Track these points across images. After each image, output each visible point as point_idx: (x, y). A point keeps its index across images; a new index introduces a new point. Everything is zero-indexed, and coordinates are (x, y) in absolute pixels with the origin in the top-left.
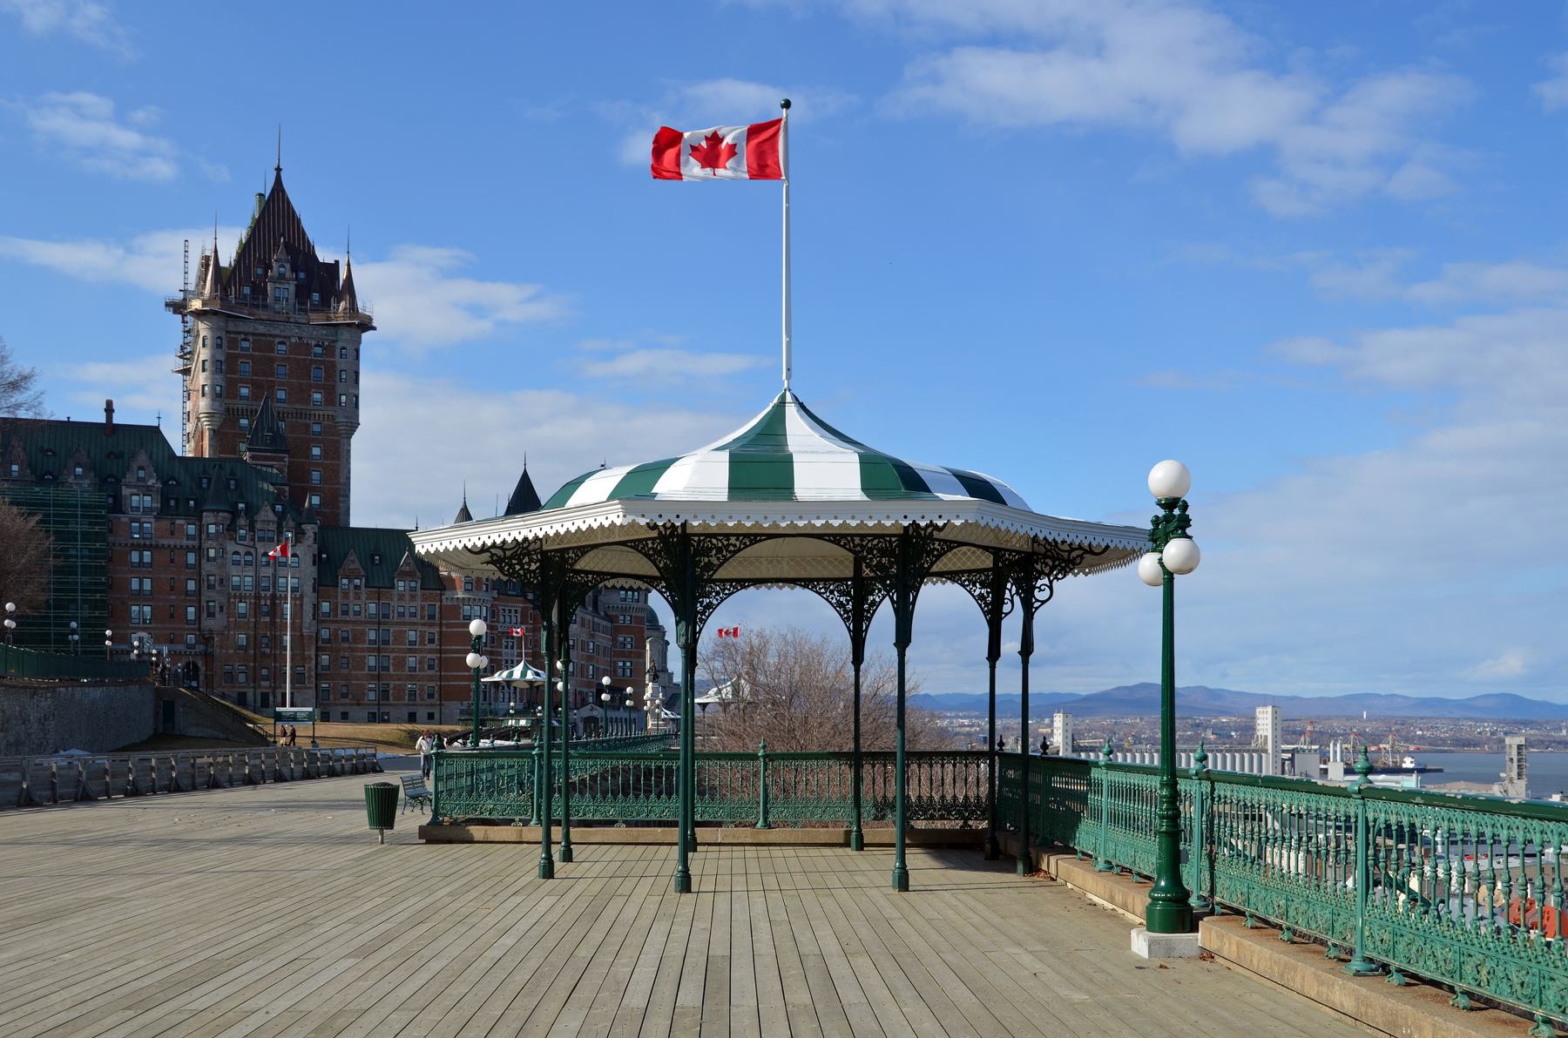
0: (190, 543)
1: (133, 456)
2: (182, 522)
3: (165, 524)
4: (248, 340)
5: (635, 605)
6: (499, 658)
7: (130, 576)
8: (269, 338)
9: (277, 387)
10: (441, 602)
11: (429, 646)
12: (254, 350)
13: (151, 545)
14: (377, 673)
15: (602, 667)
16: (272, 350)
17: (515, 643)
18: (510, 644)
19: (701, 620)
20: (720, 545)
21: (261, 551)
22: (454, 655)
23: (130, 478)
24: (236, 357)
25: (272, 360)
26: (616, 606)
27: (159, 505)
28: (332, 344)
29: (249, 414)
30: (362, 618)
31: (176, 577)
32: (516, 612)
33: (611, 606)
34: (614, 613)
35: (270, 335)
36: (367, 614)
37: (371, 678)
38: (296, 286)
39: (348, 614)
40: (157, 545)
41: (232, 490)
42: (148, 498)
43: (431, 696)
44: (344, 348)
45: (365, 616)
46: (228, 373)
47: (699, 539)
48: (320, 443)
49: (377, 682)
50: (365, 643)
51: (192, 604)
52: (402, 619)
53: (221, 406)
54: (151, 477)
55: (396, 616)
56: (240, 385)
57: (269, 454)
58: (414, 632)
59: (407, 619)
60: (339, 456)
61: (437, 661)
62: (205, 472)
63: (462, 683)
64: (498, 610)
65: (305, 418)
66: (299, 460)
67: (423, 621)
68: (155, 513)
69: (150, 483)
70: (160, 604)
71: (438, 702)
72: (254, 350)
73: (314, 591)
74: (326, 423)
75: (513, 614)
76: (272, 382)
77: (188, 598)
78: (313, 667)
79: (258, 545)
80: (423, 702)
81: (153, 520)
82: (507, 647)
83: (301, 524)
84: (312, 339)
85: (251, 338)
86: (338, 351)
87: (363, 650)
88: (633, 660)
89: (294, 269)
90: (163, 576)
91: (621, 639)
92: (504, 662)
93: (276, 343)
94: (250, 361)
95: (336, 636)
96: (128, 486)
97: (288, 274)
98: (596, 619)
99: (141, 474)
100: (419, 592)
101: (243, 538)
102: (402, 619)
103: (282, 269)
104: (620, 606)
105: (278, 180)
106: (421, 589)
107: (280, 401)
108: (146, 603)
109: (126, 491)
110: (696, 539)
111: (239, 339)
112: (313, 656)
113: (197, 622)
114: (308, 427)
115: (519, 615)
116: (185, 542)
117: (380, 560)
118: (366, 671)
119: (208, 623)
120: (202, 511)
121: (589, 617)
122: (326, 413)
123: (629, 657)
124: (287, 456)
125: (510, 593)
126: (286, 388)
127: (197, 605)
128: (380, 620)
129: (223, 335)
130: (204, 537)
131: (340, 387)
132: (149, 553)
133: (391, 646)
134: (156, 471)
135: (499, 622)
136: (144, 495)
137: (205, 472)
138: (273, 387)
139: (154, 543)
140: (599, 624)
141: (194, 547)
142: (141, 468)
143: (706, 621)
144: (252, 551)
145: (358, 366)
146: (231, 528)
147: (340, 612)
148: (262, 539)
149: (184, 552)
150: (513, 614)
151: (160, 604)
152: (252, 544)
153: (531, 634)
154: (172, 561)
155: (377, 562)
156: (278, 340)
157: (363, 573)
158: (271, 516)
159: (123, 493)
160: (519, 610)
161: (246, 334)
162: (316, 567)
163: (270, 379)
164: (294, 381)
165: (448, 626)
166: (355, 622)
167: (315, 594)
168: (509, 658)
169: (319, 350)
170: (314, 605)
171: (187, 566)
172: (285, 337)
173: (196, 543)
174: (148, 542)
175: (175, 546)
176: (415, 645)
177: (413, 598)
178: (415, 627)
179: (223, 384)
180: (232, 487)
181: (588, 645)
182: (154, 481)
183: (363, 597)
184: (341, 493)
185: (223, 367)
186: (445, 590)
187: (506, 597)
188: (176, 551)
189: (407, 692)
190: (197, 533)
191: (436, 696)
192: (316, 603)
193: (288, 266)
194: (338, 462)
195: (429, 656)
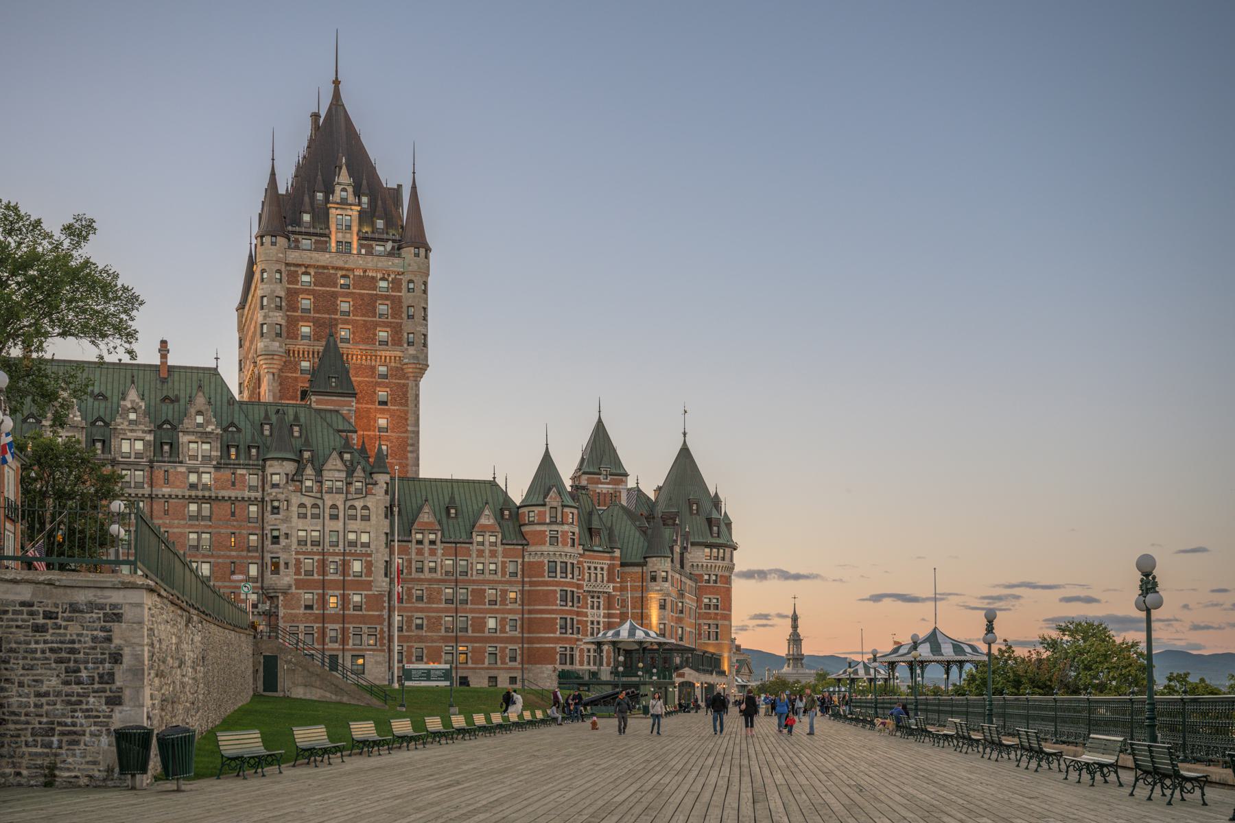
0: (253, 495)
1: (191, 400)
2: (244, 472)
3: (226, 474)
4: (309, 274)
5: (720, 563)
6: (585, 619)
7: (188, 530)
8: (331, 271)
9: (340, 326)
10: (523, 557)
11: (509, 607)
12: (315, 285)
13: (210, 497)
14: (454, 634)
15: (688, 629)
16: (335, 285)
17: (602, 603)
18: (596, 604)
21: (329, 503)
22: (539, 616)
23: (187, 424)
24: (296, 293)
25: (334, 296)
26: (700, 564)
27: (219, 454)
28: (398, 277)
29: (311, 356)
30: (438, 576)
31: (237, 531)
32: (602, 569)
33: (695, 564)
34: (697, 572)
35: (333, 268)
36: (443, 571)
37: (444, 639)
38: (359, 212)
39: (422, 572)
40: (217, 497)
41: (297, 437)
42: (206, 447)
43: (513, 659)
44: (410, 281)
45: (442, 573)
46: (288, 311)
48: (387, 387)
49: (454, 644)
50: (441, 603)
51: (254, 561)
52: (481, 577)
53: (280, 347)
54: (208, 422)
55: (474, 573)
56: (301, 324)
57: (335, 398)
58: (494, 591)
59: (487, 577)
60: (407, 401)
61: (519, 623)
62: (267, 416)
63: (547, 645)
64: (583, 566)
65: (371, 360)
66: (364, 406)
67: (503, 579)
68: (214, 463)
69: (209, 429)
70: (220, 560)
71: (520, 666)
72: (315, 285)
73: (387, 546)
74: (393, 364)
75: (599, 571)
76: (335, 319)
77: (250, 554)
78: (386, 629)
79: (326, 497)
80: (505, 666)
81: (212, 470)
82: (592, 608)
83: (371, 474)
84: (377, 271)
85: (312, 272)
86: (404, 284)
87: (437, 610)
88: (720, 622)
89: (358, 194)
90: (223, 531)
91: (706, 601)
92: (589, 624)
93: (339, 275)
94: (311, 297)
95: (410, 595)
96: (186, 432)
97: (351, 199)
98: (683, 579)
99: (200, 419)
100: (500, 549)
101: (310, 489)
102: (481, 577)
103: (344, 194)
104: (705, 565)
105: (337, 95)
106: (502, 544)
107: (343, 340)
108: (206, 560)
109: (184, 439)
111: (300, 273)
112: (386, 616)
113: (260, 579)
114: (373, 368)
115: (605, 573)
116: (247, 494)
117: (456, 514)
118: (443, 633)
119: (270, 579)
120: (264, 460)
121: (677, 576)
122: (392, 354)
123: (714, 619)
124: (354, 399)
125: (595, 548)
126: (350, 327)
127: (260, 562)
128: (456, 578)
129: (283, 269)
130: (267, 487)
131: (408, 326)
132: (208, 505)
133: (469, 606)
134: (215, 417)
135: (584, 580)
136: (203, 443)
137: (267, 416)
138: (336, 325)
139: (213, 495)
140: (686, 583)
141: (256, 498)
142: (199, 413)
144: (320, 502)
145: (426, 301)
146: (296, 478)
147: (414, 570)
148: (330, 491)
149: (247, 504)
150: (599, 571)
151: (220, 560)
152: (319, 495)
153: (618, 593)
154: (233, 514)
155: (453, 515)
156: (340, 273)
157: (438, 527)
158: (340, 465)
159: (180, 440)
160: (606, 567)
161: (307, 267)
162: (388, 521)
163: (333, 316)
164: (358, 318)
165: (531, 584)
166: (430, 581)
167: (388, 550)
168: (596, 619)
169: (383, 284)
170: (387, 562)
171: (249, 519)
172: (347, 270)
173: (259, 495)
174: (207, 494)
175: (236, 498)
176: (496, 604)
177: (493, 554)
178: (495, 586)
179: (283, 322)
180: (296, 434)
181: (677, 605)
182: (213, 427)
183: (440, 552)
184: (410, 442)
185: (283, 304)
186: (527, 545)
187: (591, 553)
188: (237, 503)
189: (487, 655)
190: (260, 484)
191: (519, 658)
192: (388, 559)
193: (350, 189)
194: (406, 408)
195: (510, 617)
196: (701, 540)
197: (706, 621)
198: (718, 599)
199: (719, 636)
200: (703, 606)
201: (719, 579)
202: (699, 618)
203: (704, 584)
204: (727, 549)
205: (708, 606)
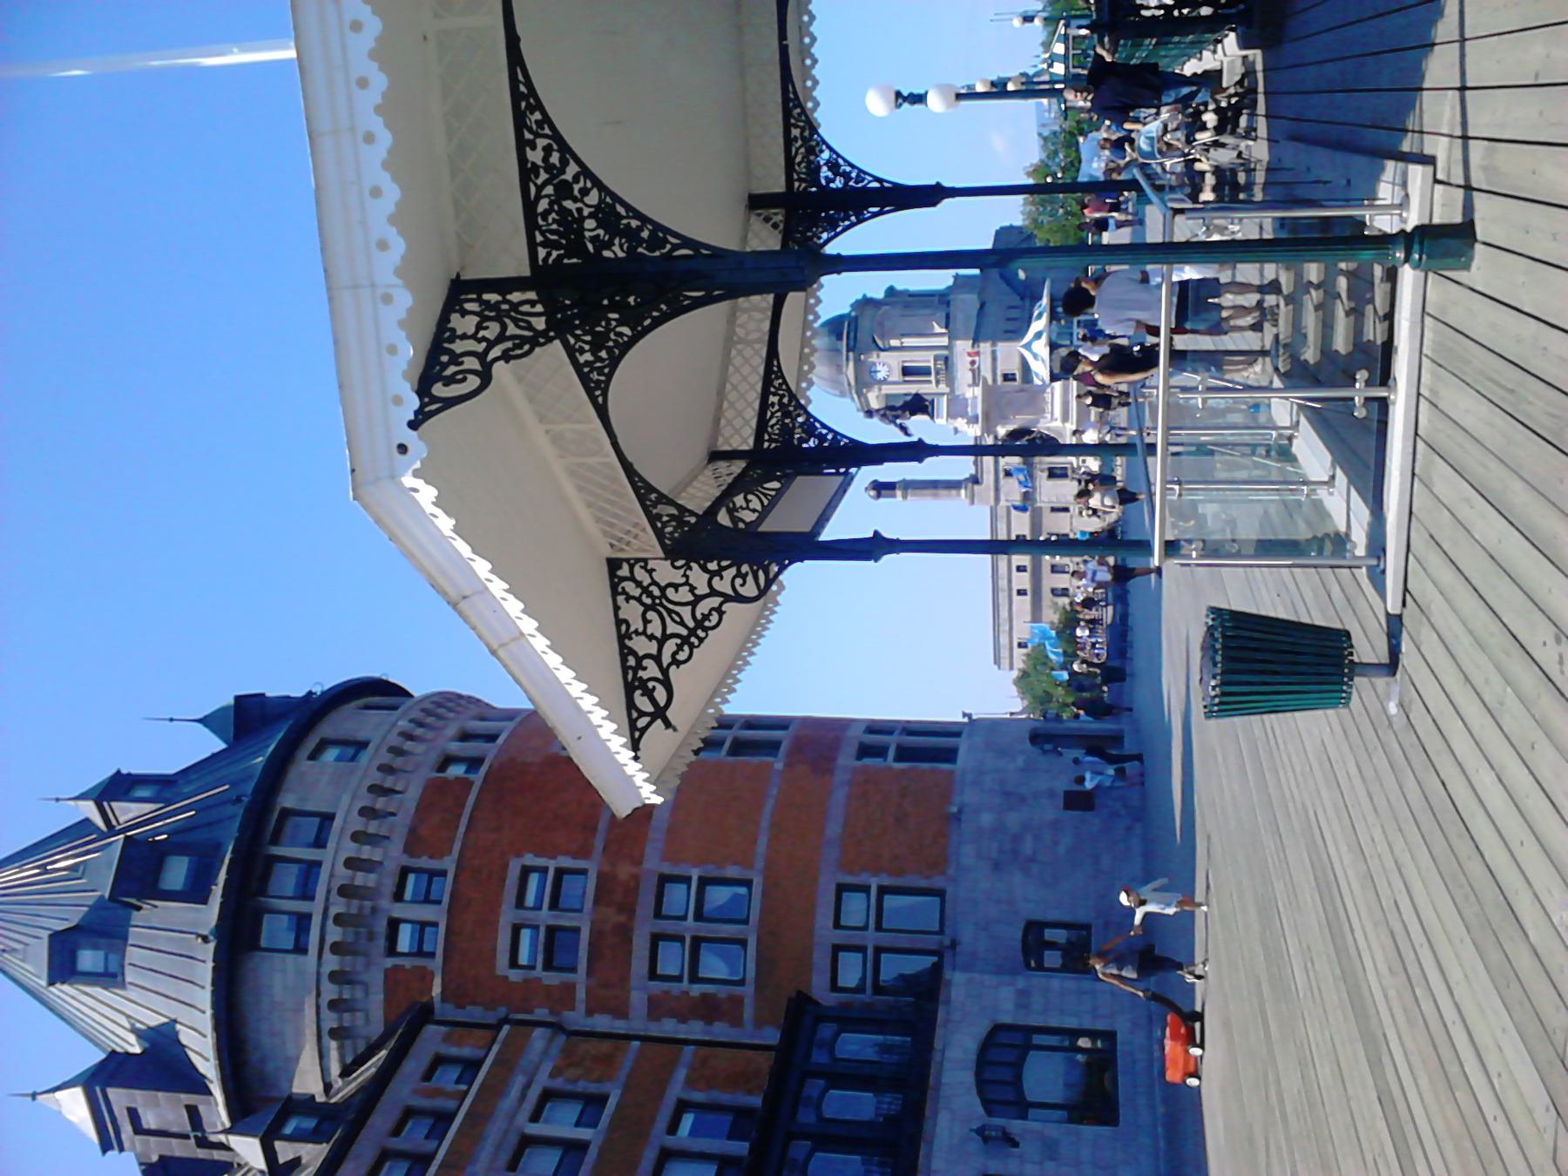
5: (339, 849)
19: (859, 180)
20: (549, 190)
26: (330, 991)
34: (376, 1000)
47: (544, 245)
88: (654, 863)
104: (332, 962)
110: (542, 253)
123: (629, 909)
143: (861, 171)
197: (639, 965)
198: (526, 872)
199: (732, 872)
200: (553, 979)
201: (424, 862)
202: (621, 1012)
204: (287, 800)
205: (555, 945)
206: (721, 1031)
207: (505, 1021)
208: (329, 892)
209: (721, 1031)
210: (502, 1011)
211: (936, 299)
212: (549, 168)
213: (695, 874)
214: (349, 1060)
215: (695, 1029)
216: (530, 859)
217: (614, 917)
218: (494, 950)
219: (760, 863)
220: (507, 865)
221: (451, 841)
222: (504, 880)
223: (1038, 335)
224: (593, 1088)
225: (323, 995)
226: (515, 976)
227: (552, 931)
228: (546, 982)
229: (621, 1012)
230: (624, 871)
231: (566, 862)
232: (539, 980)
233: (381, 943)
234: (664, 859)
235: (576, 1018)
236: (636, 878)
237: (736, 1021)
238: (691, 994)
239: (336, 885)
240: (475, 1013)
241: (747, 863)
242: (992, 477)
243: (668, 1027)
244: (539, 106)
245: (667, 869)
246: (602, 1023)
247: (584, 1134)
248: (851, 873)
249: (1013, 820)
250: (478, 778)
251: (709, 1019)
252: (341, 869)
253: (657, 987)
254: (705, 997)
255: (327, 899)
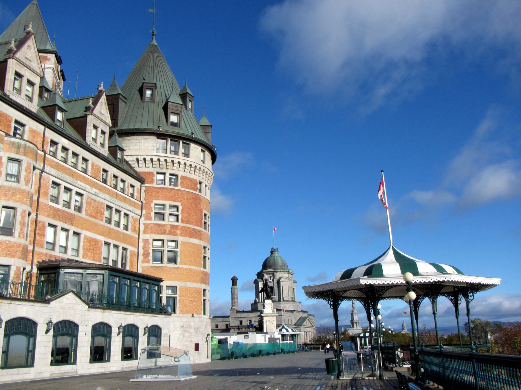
33: (141, 158)
88: (180, 239)
104: (155, 159)
123: (170, 233)
196: (151, 126)
198: (177, 207)
200: (152, 214)
201: (179, 181)
202: (145, 232)
203: (155, 185)
204: (192, 145)
206: (141, 258)
207: (142, 203)
208: (172, 158)
209: (141, 258)
210: (144, 202)
211: (293, 297)
212: (384, 289)
213: (178, 250)
214: (130, 162)
215: (141, 251)
216: (180, 208)
217: (168, 229)
218: (159, 200)
219: (181, 266)
220: (179, 202)
221: (184, 187)
222: (176, 201)
223: (287, 330)
224: (130, 227)
225: (147, 156)
226: (153, 205)
227: (164, 214)
228: (151, 213)
229: (145, 232)
230: (178, 232)
231: (180, 217)
232: (152, 211)
233: (160, 171)
234: (181, 242)
235: (143, 220)
236: (177, 235)
237: (143, 262)
238: (150, 250)
239: (174, 159)
240: (143, 195)
241: (181, 263)
242: (239, 316)
243: (141, 244)
244: (390, 288)
245: (179, 243)
246: (142, 227)
247: (61, 202)
248: (179, 290)
249: (192, 330)
250: (198, 193)
251: (143, 255)
252: (178, 160)
253: (151, 241)
254: (149, 253)
255: (170, 157)
